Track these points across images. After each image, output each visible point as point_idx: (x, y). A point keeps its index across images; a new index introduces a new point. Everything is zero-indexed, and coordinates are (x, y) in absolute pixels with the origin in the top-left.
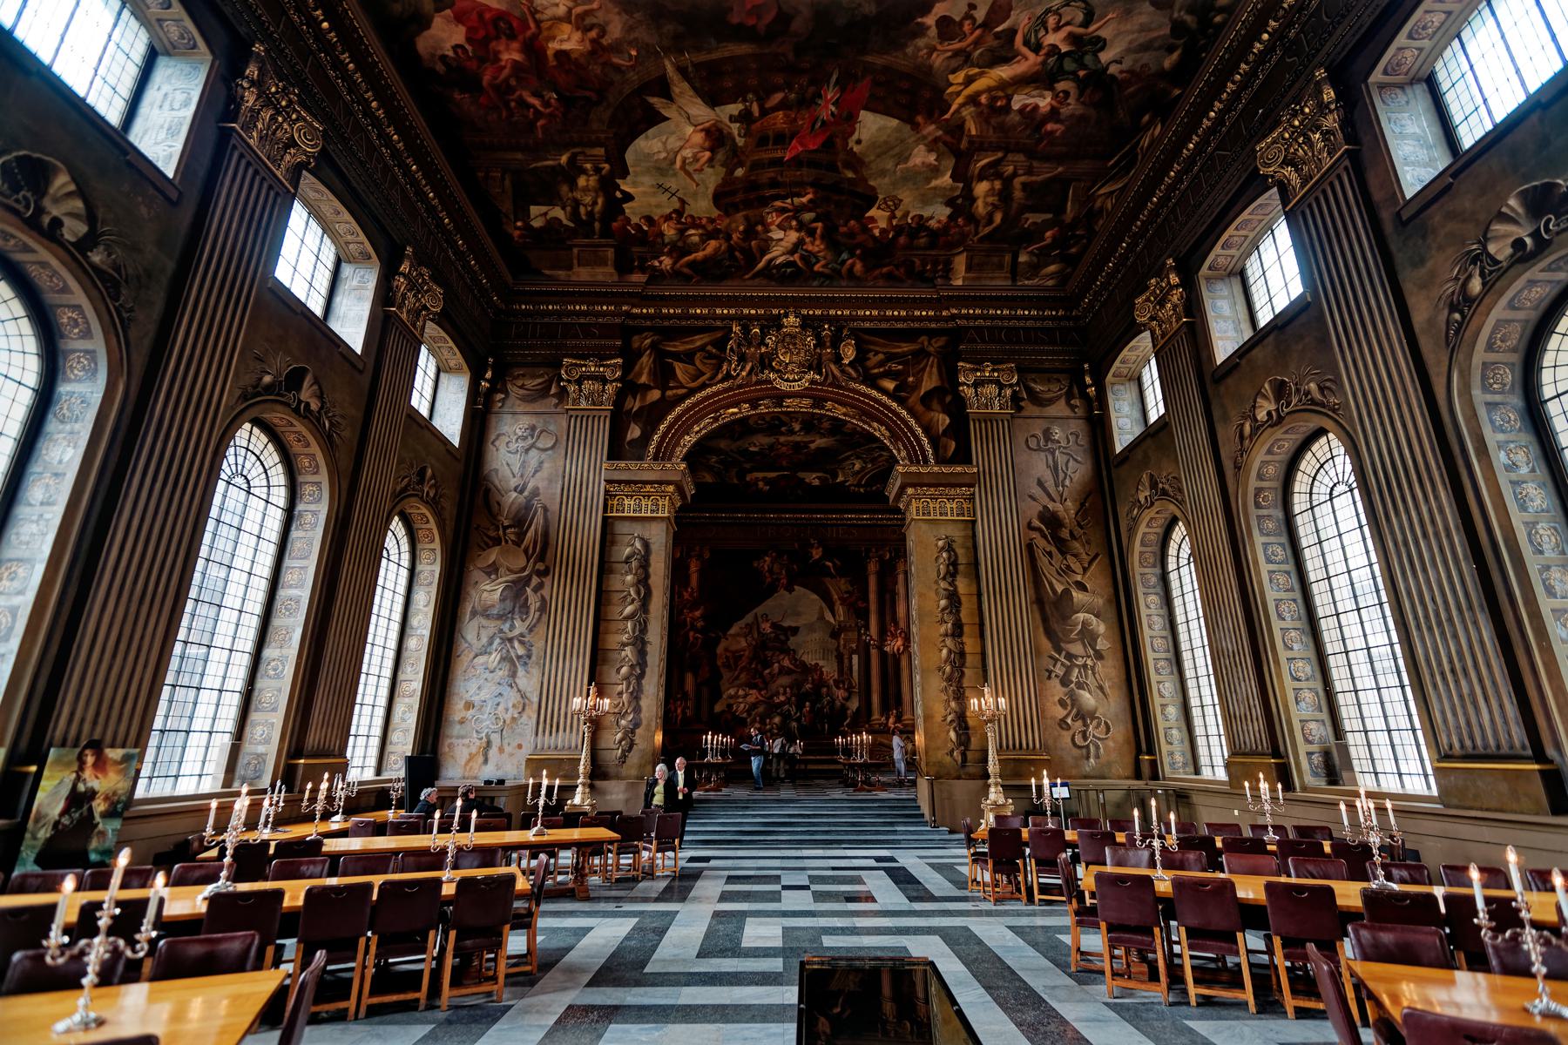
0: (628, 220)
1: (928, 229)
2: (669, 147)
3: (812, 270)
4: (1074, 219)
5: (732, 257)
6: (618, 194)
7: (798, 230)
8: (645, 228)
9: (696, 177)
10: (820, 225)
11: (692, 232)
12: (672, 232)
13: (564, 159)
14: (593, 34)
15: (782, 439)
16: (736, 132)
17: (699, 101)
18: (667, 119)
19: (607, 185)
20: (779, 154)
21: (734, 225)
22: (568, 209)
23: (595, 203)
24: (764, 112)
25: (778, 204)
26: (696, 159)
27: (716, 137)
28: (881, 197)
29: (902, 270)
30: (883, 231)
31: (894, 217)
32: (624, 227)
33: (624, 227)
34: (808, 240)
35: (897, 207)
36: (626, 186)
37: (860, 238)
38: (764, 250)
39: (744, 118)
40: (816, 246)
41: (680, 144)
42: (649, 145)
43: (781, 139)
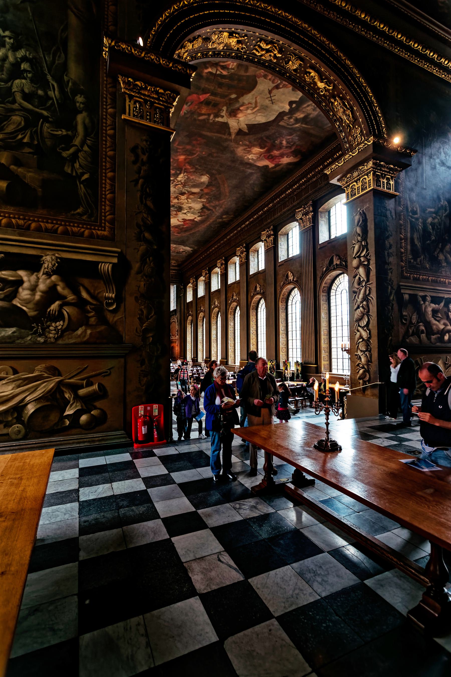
2: (255, 116)
9: (254, 101)
13: (297, 125)
14: (248, 149)
16: (224, 112)
17: (230, 126)
18: (246, 125)
19: (292, 112)
20: (212, 97)
24: (209, 115)
25: (225, 73)
26: (247, 108)
27: (233, 113)
36: (287, 108)
39: (217, 116)
41: (248, 116)
42: (261, 119)
43: (207, 103)
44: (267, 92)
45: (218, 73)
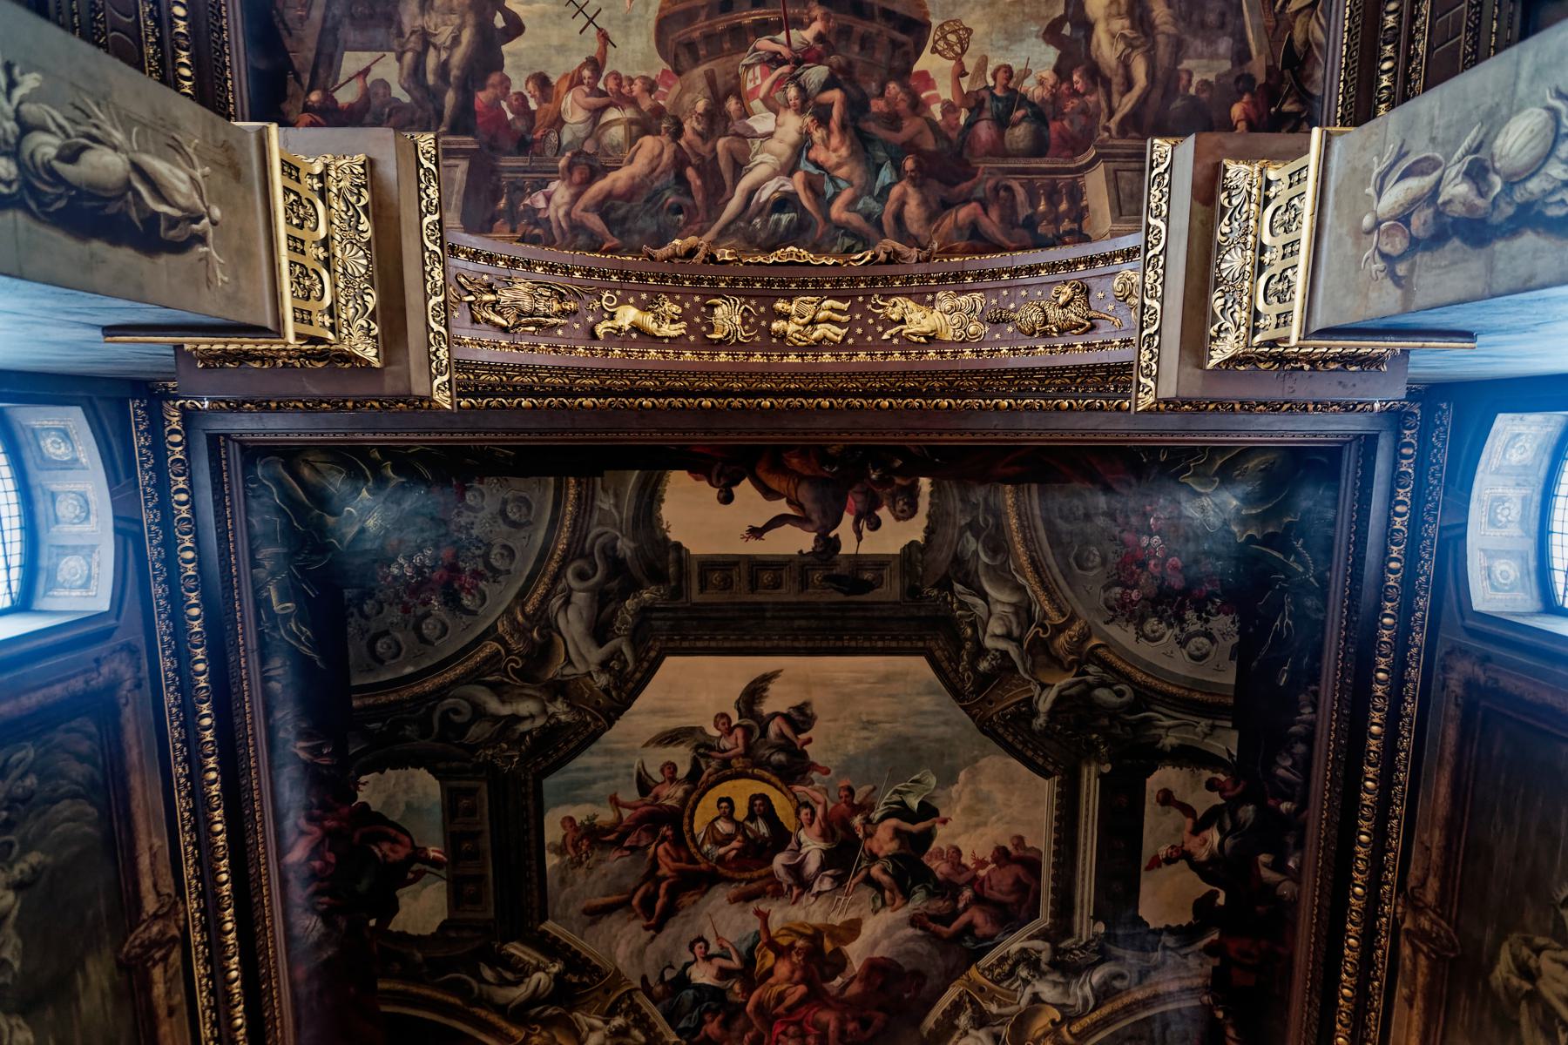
0: (506, 82)
1: (1024, 100)
3: (827, 218)
4: (1270, 71)
5: (681, 179)
6: (499, 21)
7: (801, 111)
8: (533, 105)
10: (835, 95)
11: (612, 114)
12: (580, 115)
15: (781, 915)
21: (687, 98)
22: (409, 56)
23: (456, 40)
25: (764, 44)
28: (935, 22)
29: (994, 214)
30: (949, 108)
31: (963, 74)
32: (494, 105)
33: (494, 105)
34: (818, 135)
35: (964, 45)
37: (910, 127)
38: (739, 167)
40: (833, 151)
44: (615, 35)
45: (782, 37)
